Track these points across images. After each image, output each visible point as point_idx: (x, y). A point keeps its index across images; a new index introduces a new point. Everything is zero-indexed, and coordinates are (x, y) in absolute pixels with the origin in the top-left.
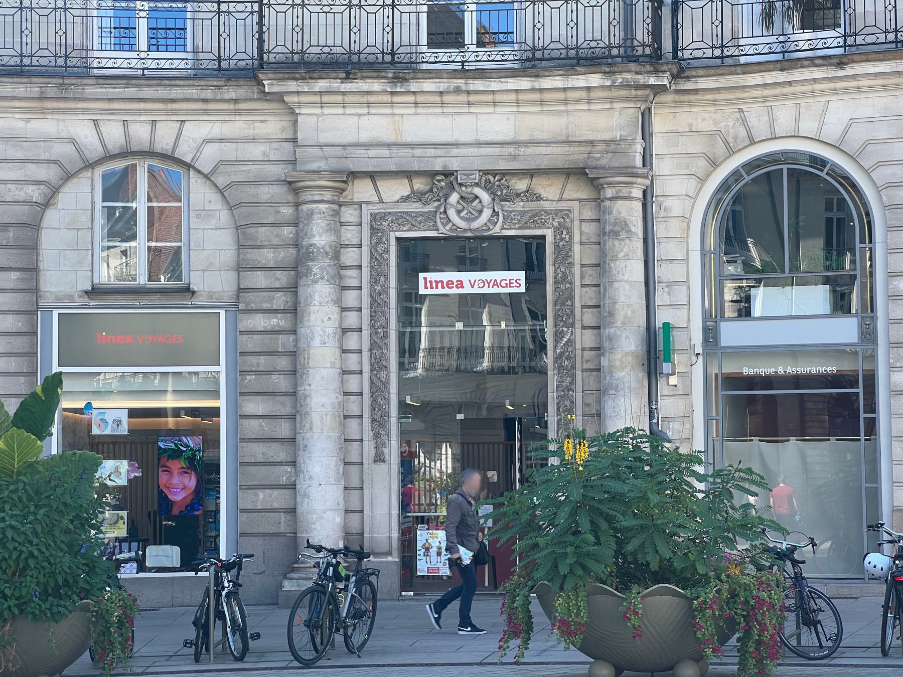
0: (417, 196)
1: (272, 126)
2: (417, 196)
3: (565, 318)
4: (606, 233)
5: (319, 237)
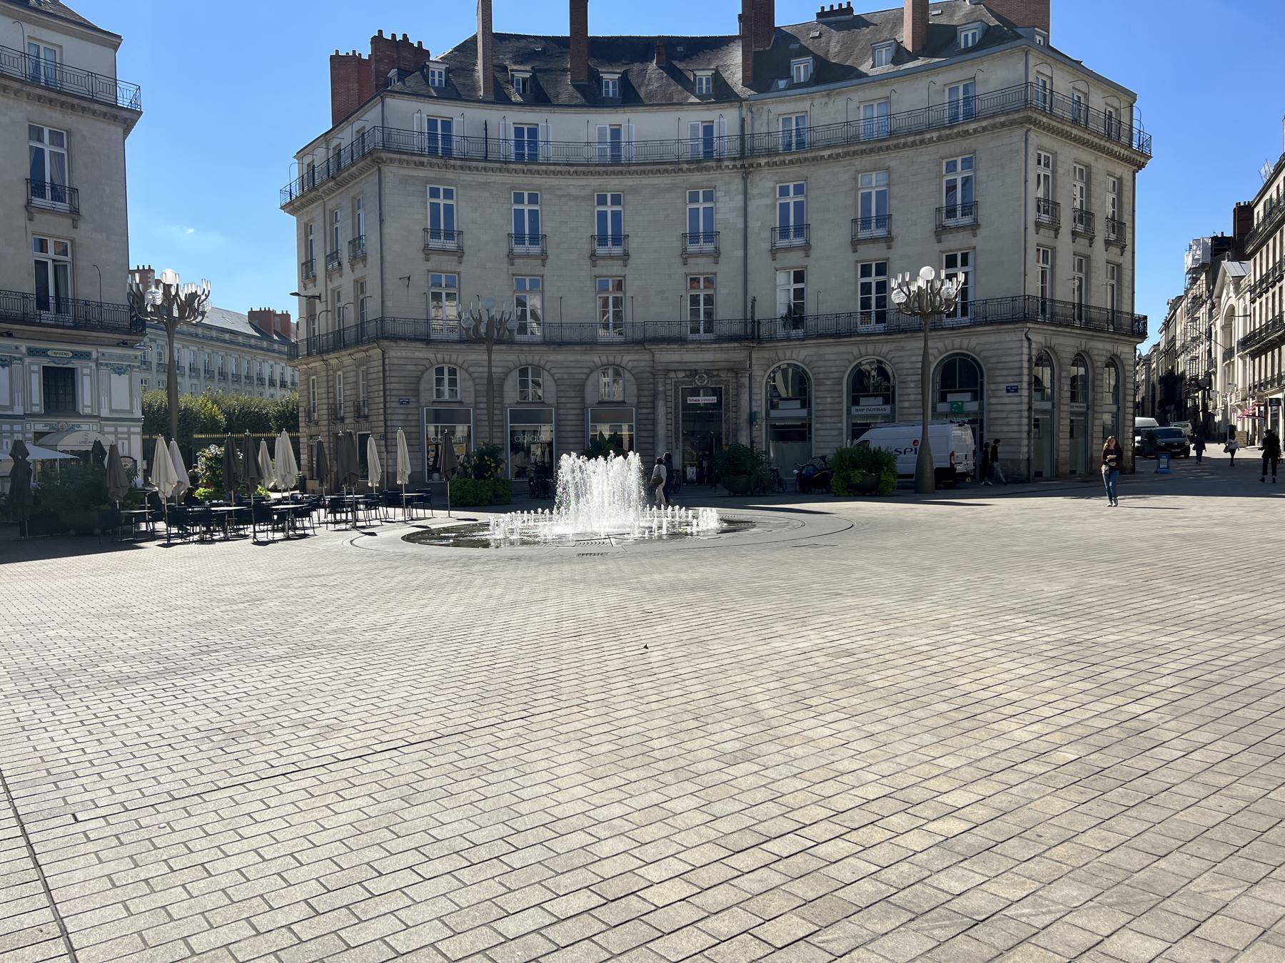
0: (687, 376)
1: (647, 357)
2: (687, 376)
3: (727, 410)
4: (739, 386)
5: (661, 388)
